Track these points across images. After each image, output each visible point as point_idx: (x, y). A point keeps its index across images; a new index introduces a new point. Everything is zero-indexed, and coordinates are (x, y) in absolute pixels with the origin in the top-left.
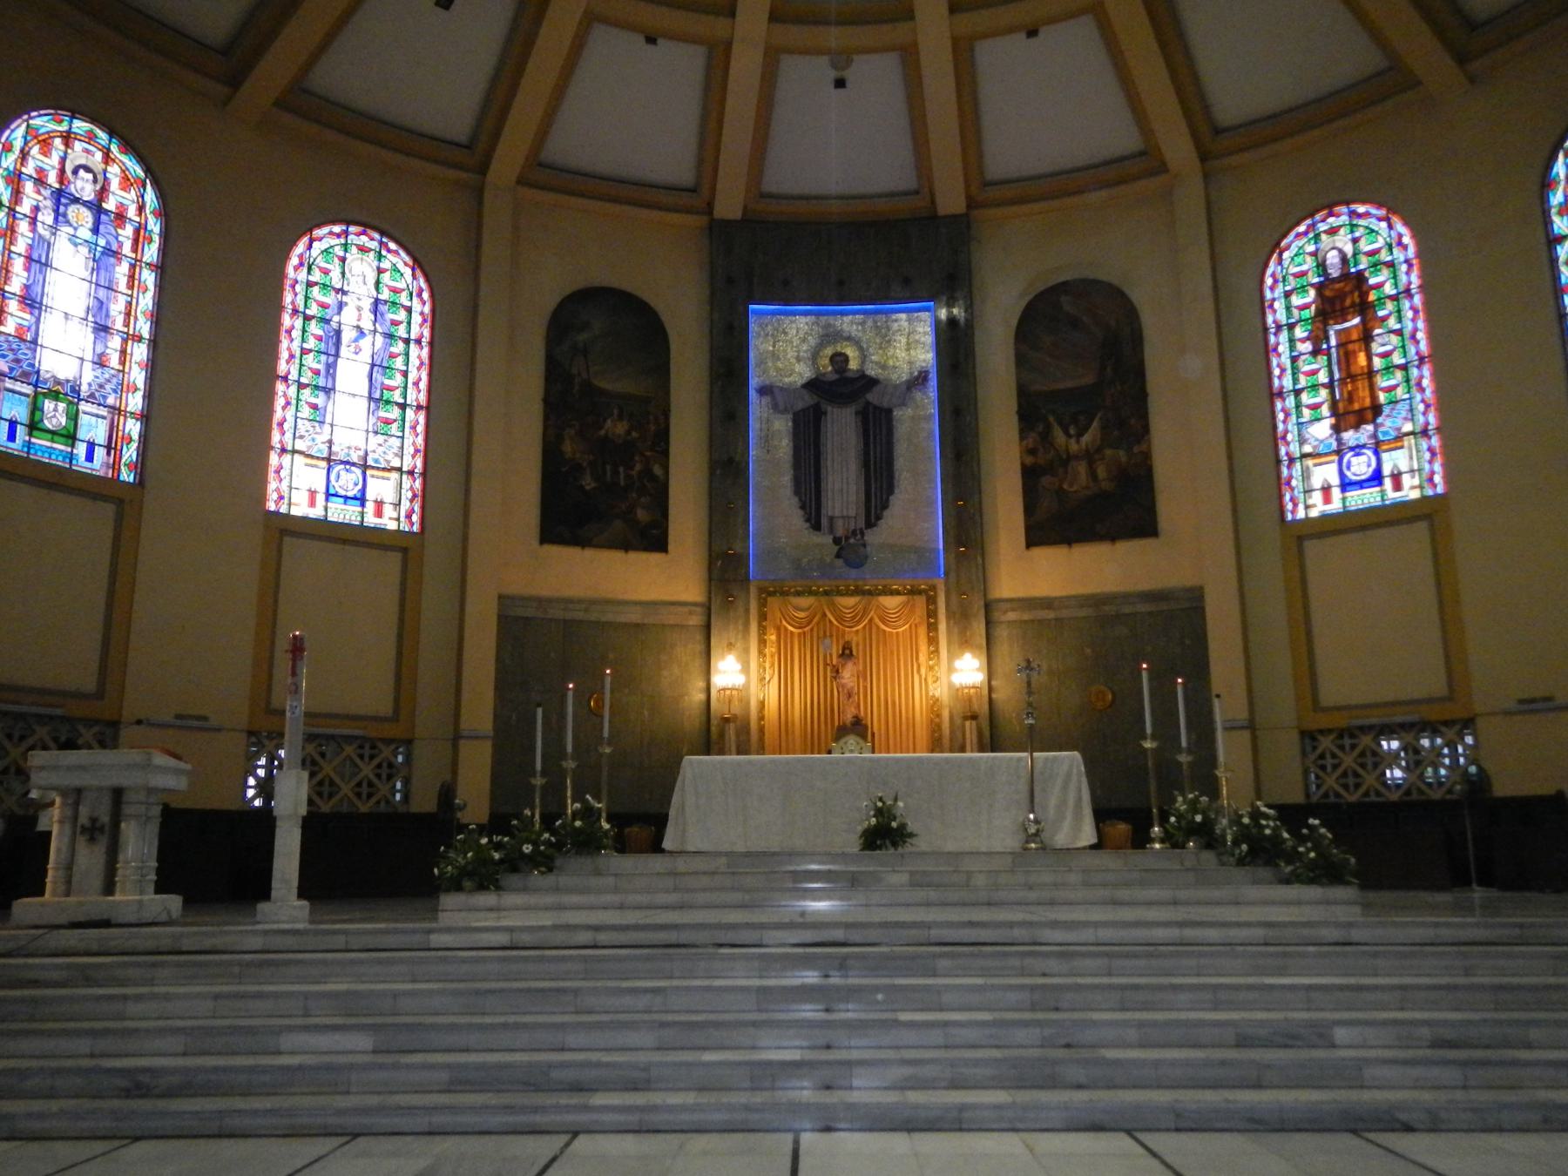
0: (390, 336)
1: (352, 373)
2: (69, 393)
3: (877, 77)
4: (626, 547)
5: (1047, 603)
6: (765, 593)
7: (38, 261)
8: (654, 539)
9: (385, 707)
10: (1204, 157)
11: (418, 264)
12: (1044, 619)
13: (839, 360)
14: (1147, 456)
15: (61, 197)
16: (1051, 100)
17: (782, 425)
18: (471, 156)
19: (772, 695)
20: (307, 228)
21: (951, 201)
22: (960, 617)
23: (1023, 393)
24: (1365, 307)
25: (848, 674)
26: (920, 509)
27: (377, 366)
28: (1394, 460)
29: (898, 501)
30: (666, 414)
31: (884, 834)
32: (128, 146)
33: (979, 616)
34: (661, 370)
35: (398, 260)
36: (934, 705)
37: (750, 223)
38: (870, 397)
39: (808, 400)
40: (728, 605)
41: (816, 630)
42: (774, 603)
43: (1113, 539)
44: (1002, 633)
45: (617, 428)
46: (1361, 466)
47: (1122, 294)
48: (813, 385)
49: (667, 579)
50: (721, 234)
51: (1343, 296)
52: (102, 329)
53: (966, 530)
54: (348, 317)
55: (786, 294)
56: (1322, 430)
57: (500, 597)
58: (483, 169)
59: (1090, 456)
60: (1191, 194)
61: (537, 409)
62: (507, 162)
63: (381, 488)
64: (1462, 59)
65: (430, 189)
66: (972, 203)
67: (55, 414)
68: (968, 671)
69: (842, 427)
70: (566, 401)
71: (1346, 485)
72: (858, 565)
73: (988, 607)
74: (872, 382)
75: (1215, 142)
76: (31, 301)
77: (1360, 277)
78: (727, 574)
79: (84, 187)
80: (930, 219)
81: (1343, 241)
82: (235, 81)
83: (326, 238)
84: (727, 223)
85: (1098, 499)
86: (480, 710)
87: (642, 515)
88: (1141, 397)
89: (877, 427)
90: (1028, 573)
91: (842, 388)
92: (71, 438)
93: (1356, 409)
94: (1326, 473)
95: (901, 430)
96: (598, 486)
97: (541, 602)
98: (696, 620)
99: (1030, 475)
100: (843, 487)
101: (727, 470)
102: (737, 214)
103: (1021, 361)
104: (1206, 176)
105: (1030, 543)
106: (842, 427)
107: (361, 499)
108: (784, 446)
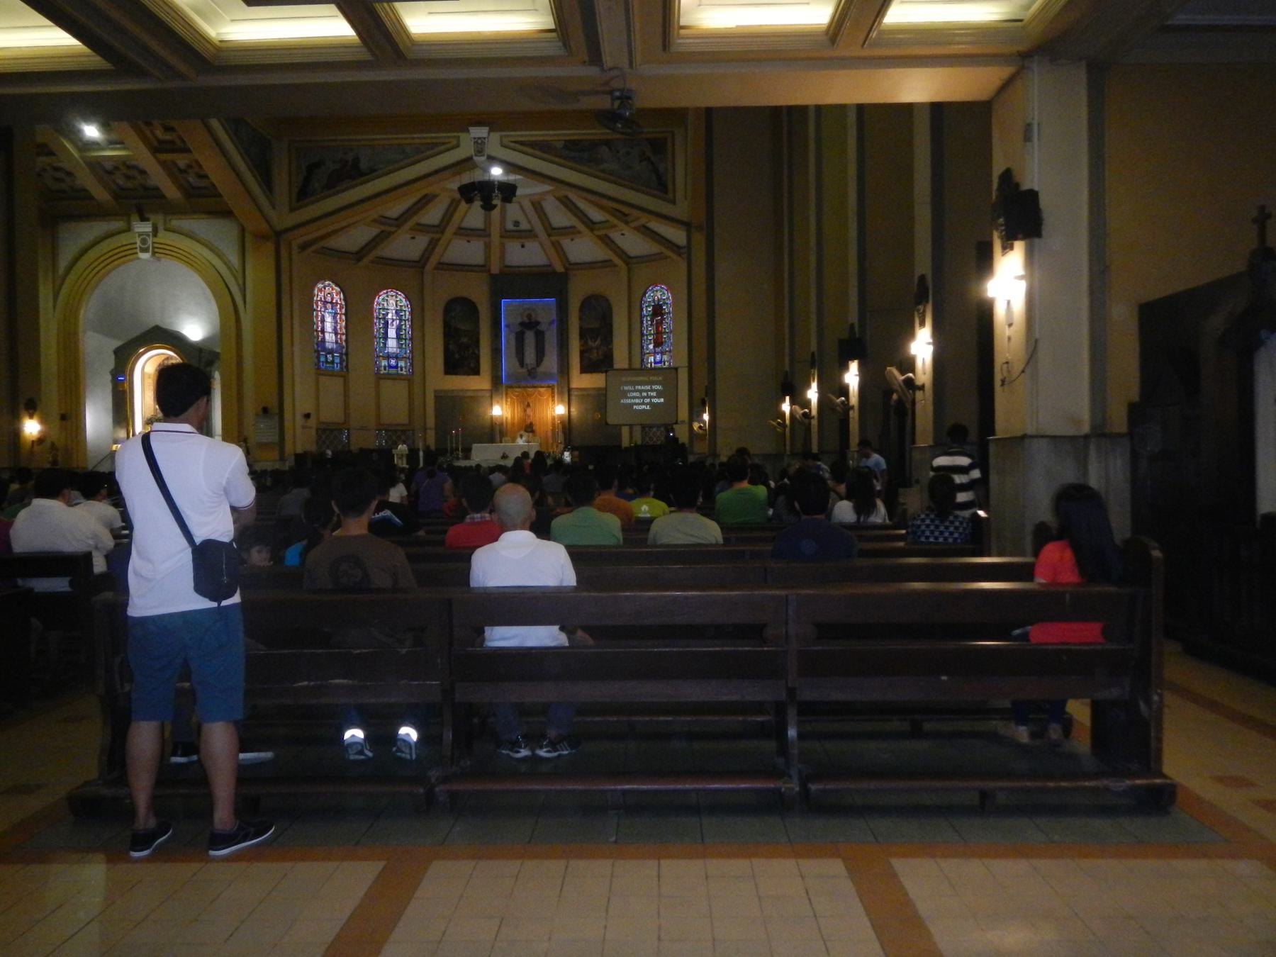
0: (401, 320)
1: (392, 333)
2: (331, 352)
3: (532, 246)
4: (468, 374)
7: (323, 321)
8: (476, 372)
9: (406, 422)
10: (627, 264)
11: (407, 298)
12: (585, 394)
13: (529, 316)
15: (325, 303)
16: (583, 249)
17: (513, 337)
18: (419, 265)
20: (377, 293)
21: (559, 268)
22: (561, 393)
23: (581, 328)
24: (662, 315)
25: (529, 411)
26: (551, 362)
27: (399, 329)
28: (665, 357)
29: (546, 359)
30: (478, 333)
31: (504, 457)
32: (337, 285)
33: (568, 394)
35: (401, 297)
36: (553, 418)
38: (539, 328)
39: (519, 329)
44: (573, 398)
45: (465, 340)
46: (658, 357)
47: (607, 300)
48: (522, 324)
49: (481, 383)
50: (494, 279)
51: (658, 310)
52: (336, 334)
53: (564, 370)
54: (390, 316)
56: (651, 347)
58: (423, 267)
59: (597, 348)
61: (441, 336)
62: (429, 267)
63: (402, 364)
66: (566, 269)
67: (329, 357)
68: (560, 410)
69: (530, 337)
70: (450, 333)
72: (534, 378)
73: (569, 390)
74: (538, 323)
76: (323, 331)
78: (496, 382)
79: (329, 299)
80: (555, 273)
81: (659, 294)
82: (359, 260)
83: (383, 295)
85: (598, 362)
86: (431, 422)
89: (540, 337)
90: (581, 381)
91: (530, 324)
92: (333, 362)
93: (658, 343)
94: (652, 359)
96: (460, 359)
97: (446, 391)
99: (582, 353)
100: (530, 357)
101: (496, 352)
103: (580, 319)
104: (629, 270)
106: (530, 337)
107: (396, 367)
108: (513, 342)
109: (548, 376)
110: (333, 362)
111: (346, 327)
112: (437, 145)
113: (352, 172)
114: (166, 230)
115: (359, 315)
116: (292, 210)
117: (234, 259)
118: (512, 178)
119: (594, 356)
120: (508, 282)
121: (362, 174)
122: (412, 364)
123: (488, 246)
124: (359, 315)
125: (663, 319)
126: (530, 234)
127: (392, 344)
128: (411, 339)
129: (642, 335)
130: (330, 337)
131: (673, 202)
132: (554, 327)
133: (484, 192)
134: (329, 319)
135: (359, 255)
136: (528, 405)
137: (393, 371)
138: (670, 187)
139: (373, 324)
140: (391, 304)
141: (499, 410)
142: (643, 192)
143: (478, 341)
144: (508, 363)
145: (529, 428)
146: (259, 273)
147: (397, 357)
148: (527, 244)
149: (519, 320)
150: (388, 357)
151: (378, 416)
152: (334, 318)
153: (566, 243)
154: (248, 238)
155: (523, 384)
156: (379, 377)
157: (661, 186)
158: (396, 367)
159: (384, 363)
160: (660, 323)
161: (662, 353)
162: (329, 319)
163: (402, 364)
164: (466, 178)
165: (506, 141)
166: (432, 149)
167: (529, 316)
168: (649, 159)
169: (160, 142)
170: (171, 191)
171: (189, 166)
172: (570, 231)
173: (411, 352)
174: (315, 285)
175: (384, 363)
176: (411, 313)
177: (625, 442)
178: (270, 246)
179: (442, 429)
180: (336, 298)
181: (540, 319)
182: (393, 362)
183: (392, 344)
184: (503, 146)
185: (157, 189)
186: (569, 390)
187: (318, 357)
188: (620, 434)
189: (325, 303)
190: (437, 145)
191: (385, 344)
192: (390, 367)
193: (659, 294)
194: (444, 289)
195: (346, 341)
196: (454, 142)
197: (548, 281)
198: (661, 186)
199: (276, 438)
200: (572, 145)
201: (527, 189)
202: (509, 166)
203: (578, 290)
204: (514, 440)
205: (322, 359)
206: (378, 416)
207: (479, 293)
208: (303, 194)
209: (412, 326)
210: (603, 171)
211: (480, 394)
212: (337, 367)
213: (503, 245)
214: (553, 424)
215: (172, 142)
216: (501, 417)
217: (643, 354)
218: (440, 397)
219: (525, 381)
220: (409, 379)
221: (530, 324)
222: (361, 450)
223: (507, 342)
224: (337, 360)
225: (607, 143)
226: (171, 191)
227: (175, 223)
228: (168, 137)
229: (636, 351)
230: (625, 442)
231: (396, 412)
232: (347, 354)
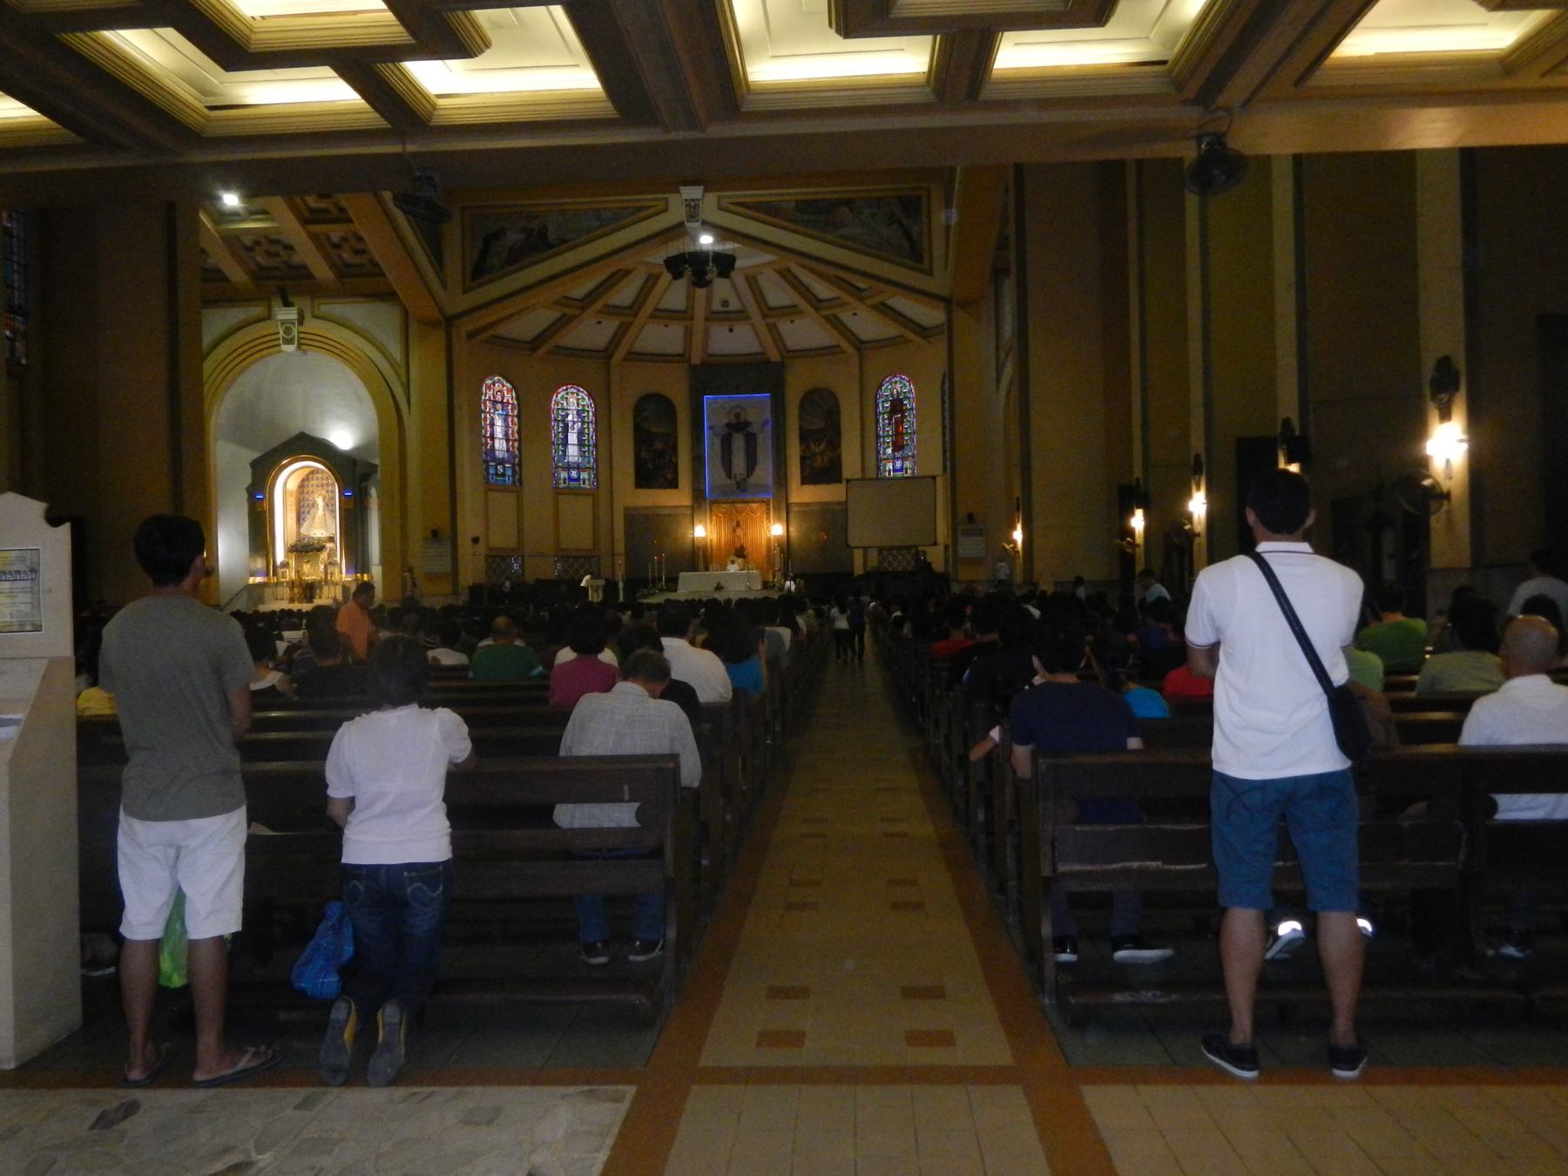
1: (573, 438)
2: (502, 462)
4: (664, 487)
5: (807, 504)
6: (713, 503)
7: (492, 425)
8: (674, 484)
10: (858, 349)
11: (590, 395)
12: (807, 510)
13: (737, 415)
14: (839, 457)
15: (495, 402)
16: (805, 332)
17: (717, 441)
18: (606, 353)
19: (714, 537)
20: (555, 390)
21: (774, 356)
22: (777, 509)
23: (801, 429)
24: (903, 412)
25: (739, 532)
26: (765, 471)
27: (581, 433)
28: (907, 464)
31: (719, 588)
33: (785, 510)
34: (673, 422)
35: (583, 394)
36: (769, 540)
37: (703, 364)
40: (700, 507)
41: (729, 516)
42: (715, 507)
43: (828, 482)
44: (792, 515)
45: (659, 446)
46: (898, 464)
48: (728, 425)
49: (678, 498)
51: (897, 406)
52: (507, 440)
53: (781, 481)
55: (717, 391)
56: (889, 451)
57: (626, 509)
59: (822, 453)
60: (855, 361)
64: (925, 337)
65: (592, 368)
68: (777, 530)
69: (739, 442)
70: (642, 437)
71: (895, 470)
73: (788, 506)
74: (748, 424)
75: (859, 344)
76: (492, 438)
77: (901, 401)
78: (699, 496)
79: (499, 398)
80: (768, 362)
81: (898, 386)
84: (695, 366)
85: (823, 471)
86: (620, 547)
87: (669, 476)
88: (838, 434)
89: (751, 441)
90: (803, 494)
91: (738, 425)
92: (503, 475)
93: (898, 446)
95: (759, 441)
96: (654, 468)
98: (689, 512)
99: (803, 459)
101: (698, 460)
102: (698, 362)
103: (801, 418)
104: (861, 357)
105: (803, 483)
106: (739, 442)
109: (761, 488)
110: (503, 475)
111: (519, 432)
112: (641, 209)
113: (539, 243)
114: (314, 317)
115: (534, 418)
116: (465, 291)
117: (396, 351)
118: (729, 247)
119: (818, 463)
120: (713, 375)
121: (550, 246)
122: (596, 476)
123: (688, 333)
124: (534, 418)
125: (903, 417)
126: (742, 315)
127: (573, 451)
128: (596, 445)
129: (878, 437)
130: (500, 445)
131: (930, 273)
132: (769, 428)
133: (695, 267)
134: (499, 422)
135: (534, 344)
136: (738, 525)
137: (573, 484)
138: (926, 256)
139: (549, 429)
140: (572, 402)
141: (701, 531)
142: (907, 267)
143: (675, 449)
144: (712, 474)
145: (740, 553)
146: (426, 368)
147: (578, 468)
148: (737, 328)
149: (726, 421)
150: (568, 467)
151: (557, 541)
152: (505, 420)
153: (785, 327)
154: (413, 327)
155: (732, 498)
156: (558, 492)
157: (914, 253)
158: (578, 479)
159: (564, 475)
160: (900, 422)
161: (904, 459)
162: (499, 422)
163: (584, 475)
164: (674, 249)
165: (724, 202)
166: (638, 213)
167: (737, 415)
168: (899, 222)
169: (311, 210)
170: (322, 271)
171: (344, 239)
172: (790, 311)
173: (596, 461)
174: (483, 381)
175: (564, 475)
176: (595, 414)
177: (858, 570)
178: (439, 336)
179: (636, 555)
180: (508, 397)
181: (750, 419)
182: (574, 474)
183: (573, 451)
184: (721, 209)
185: (304, 267)
186: (788, 506)
187: (487, 470)
188: (851, 559)
189: (495, 402)
190: (641, 209)
191: (564, 452)
192: (570, 479)
193: (898, 386)
194: (634, 384)
195: (519, 449)
196: (661, 205)
197: (761, 373)
198: (914, 253)
199: (448, 569)
200: (804, 206)
201: (747, 260)
202: (723, 232)
203: (797, 384)
204: (724, 567)
205: (492, 471)
206: (557, 541)
207: (676, 388)
208: (479, 271)
209: (595, 430)
210: (842, 237)
211: (680, 511)
212: (509, 481)
213: (707, 332)
214: (769, 548)
215: (326, 211)
216: (705, 539)
217: (879, 460)
218: (632, 517)
219: (733, 495)
220: (593, 494)
221: (738, 425)
222: (538, 581)
223: (712, 445)
224: (509, 472)
225: (848, 203)
226: (322, 271)
227: (327, 308)
228: (323, 205)
229: (870, 454)
230: (858, 570)
231: (578, 536)
232: (520, 464)
